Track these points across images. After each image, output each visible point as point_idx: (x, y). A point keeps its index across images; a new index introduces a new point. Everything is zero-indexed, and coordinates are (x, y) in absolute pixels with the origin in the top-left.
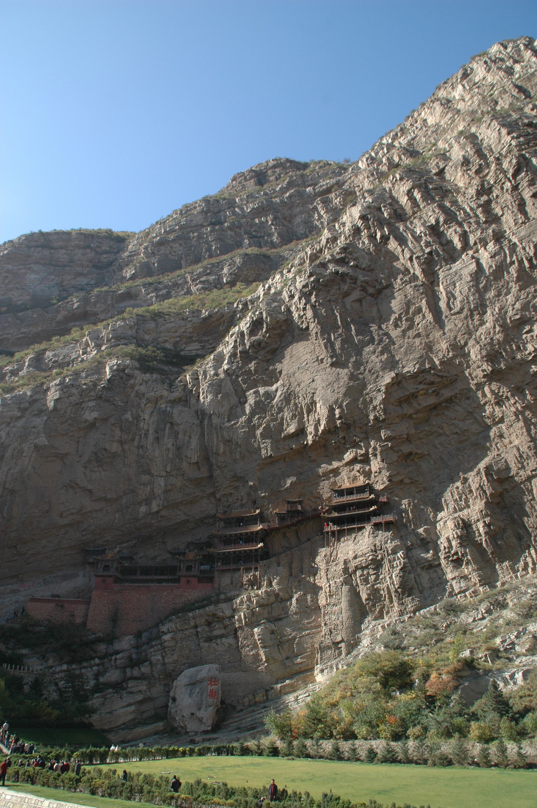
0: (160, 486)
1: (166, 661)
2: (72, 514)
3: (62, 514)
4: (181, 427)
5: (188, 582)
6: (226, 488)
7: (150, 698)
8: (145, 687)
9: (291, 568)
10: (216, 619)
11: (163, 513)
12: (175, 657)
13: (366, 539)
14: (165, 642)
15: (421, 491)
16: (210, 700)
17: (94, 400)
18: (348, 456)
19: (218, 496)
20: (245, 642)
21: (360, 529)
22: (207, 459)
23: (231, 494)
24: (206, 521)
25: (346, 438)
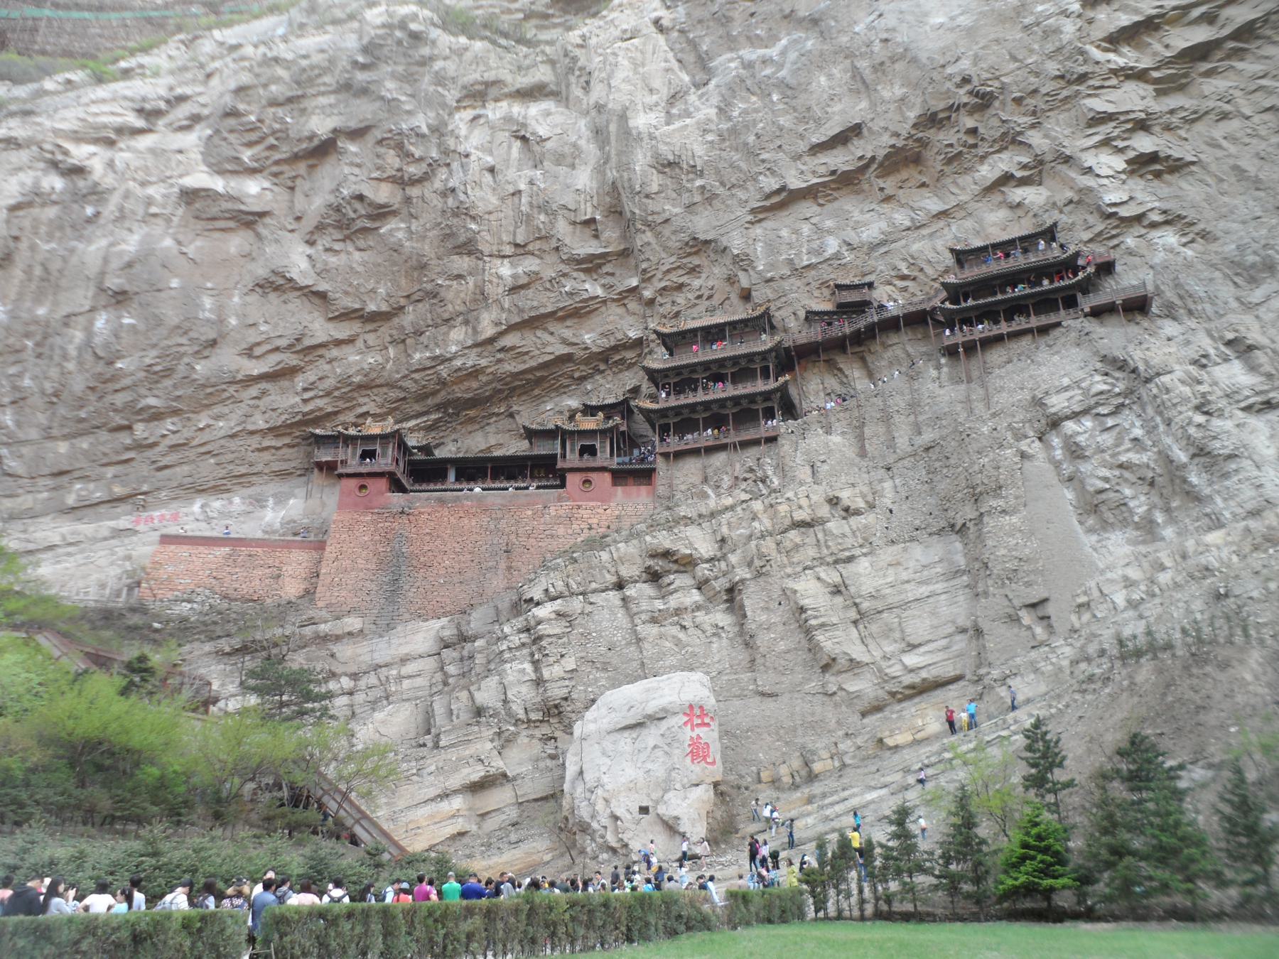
0: (500, 277)
1: (546, 674)
2: (277, 349)
3: (251, 349)
4: (549, 145)
5: (587, 482)
6: (668, 271)
7: (504, 775)
8: (489, 745)
9: (861, 438)
10: (675, 567)
11: (508, 341)
12: (570, 663)
13: (1075, 350)
14: (539, 623)
15: (1192, 241)
16: (696, 770)
17: (334, 92)
18: (987, 172)
19: (647, 294)
20: (764, 618)
21: (1044, 330)
22: (616, 211)
23: (680, 287)
24: (617, 357)
25: (981, 130)
